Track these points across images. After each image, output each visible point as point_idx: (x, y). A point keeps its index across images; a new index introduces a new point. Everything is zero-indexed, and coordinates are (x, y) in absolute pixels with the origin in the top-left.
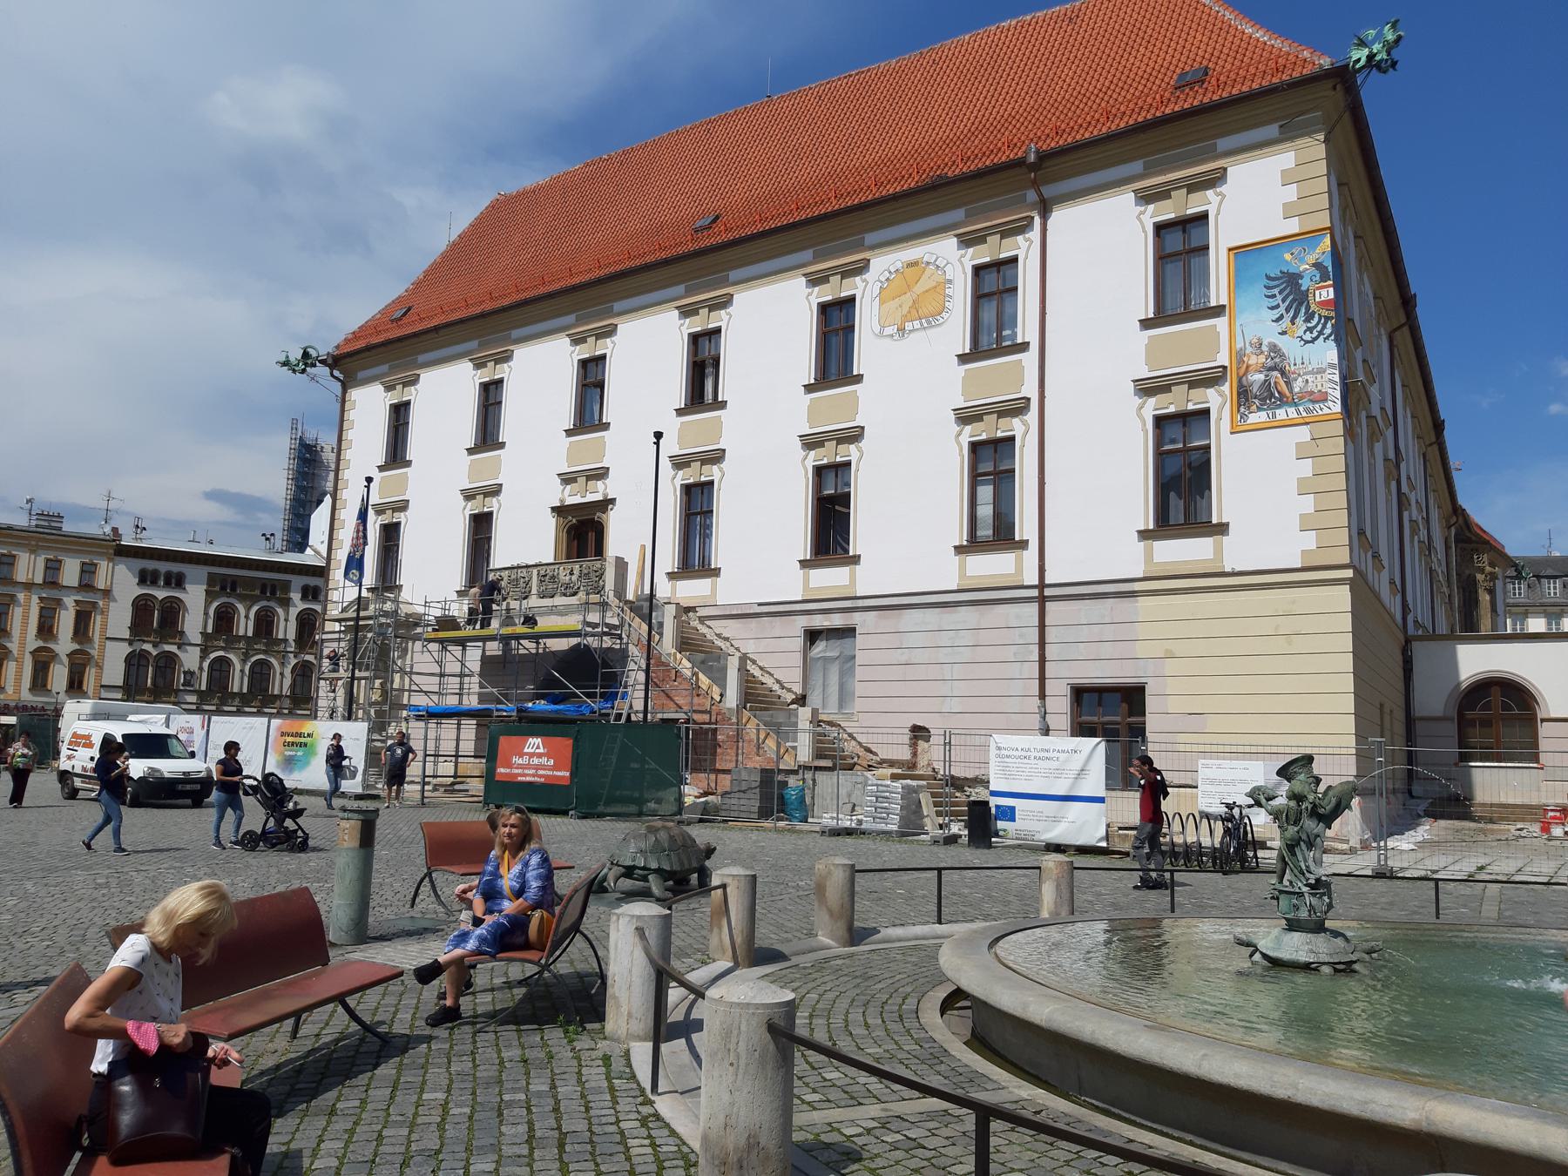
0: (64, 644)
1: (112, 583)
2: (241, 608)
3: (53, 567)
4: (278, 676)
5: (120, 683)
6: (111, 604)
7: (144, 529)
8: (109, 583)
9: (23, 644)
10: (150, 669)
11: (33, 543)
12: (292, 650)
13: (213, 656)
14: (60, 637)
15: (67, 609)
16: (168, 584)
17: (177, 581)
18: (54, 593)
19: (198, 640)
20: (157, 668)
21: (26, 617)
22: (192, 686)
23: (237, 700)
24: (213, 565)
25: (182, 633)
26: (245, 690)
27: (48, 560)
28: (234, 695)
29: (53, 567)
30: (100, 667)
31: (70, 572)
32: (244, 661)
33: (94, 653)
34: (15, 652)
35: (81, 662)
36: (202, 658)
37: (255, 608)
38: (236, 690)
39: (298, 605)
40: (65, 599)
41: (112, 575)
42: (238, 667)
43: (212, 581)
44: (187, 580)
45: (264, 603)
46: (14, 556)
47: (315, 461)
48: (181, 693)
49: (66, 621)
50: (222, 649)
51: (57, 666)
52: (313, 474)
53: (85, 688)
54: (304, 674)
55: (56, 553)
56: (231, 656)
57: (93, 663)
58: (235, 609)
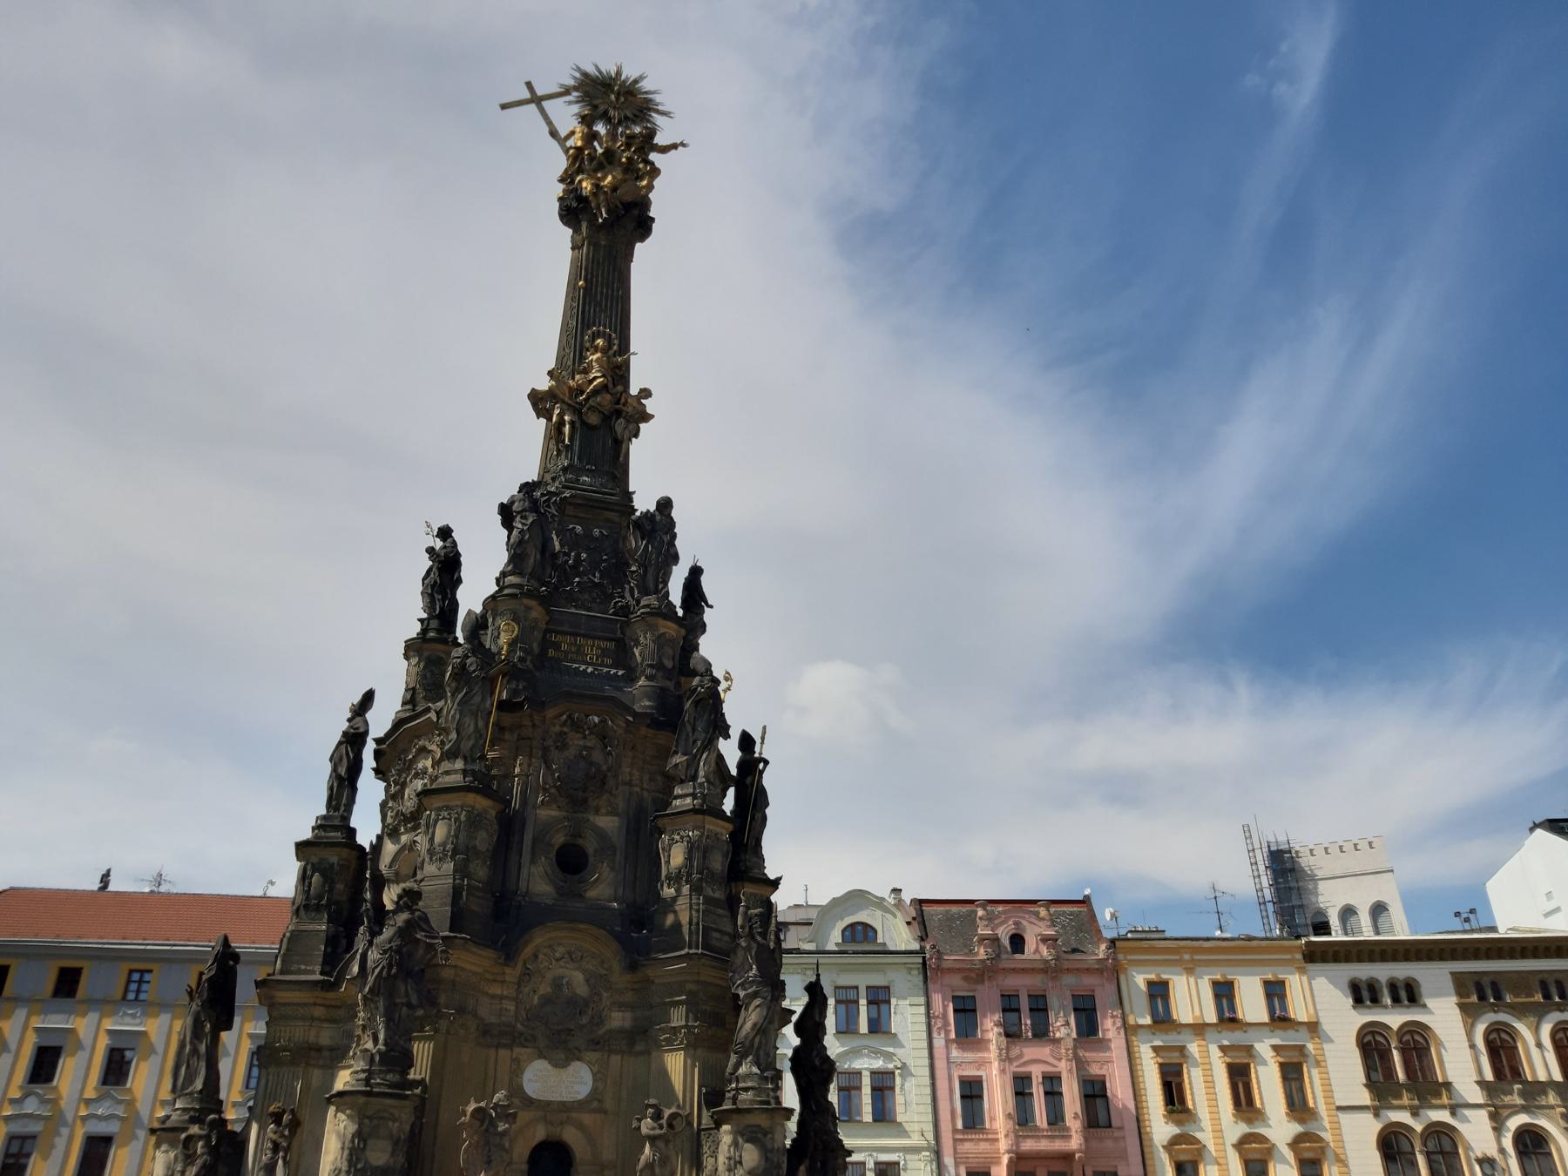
2: (1521, 1027)
3: (1224, 992)
6: (1326, 1046)
9: (1218, 1132)
11: (1187, 957)
15: (1265, 1063)
19: (1476, 1095)
21: (1210, 1083)
25: (1447, 1085)
29: (1224, 992)
31: (1251, 1003)
33: (1327, 1136)
34: (1211, 1147)
36: (1498, 1129)
43: (1462, 984)
47: (1293, 870)
55: (1225, 970)
56: (1543, 1122)
58: (1513, 1034)
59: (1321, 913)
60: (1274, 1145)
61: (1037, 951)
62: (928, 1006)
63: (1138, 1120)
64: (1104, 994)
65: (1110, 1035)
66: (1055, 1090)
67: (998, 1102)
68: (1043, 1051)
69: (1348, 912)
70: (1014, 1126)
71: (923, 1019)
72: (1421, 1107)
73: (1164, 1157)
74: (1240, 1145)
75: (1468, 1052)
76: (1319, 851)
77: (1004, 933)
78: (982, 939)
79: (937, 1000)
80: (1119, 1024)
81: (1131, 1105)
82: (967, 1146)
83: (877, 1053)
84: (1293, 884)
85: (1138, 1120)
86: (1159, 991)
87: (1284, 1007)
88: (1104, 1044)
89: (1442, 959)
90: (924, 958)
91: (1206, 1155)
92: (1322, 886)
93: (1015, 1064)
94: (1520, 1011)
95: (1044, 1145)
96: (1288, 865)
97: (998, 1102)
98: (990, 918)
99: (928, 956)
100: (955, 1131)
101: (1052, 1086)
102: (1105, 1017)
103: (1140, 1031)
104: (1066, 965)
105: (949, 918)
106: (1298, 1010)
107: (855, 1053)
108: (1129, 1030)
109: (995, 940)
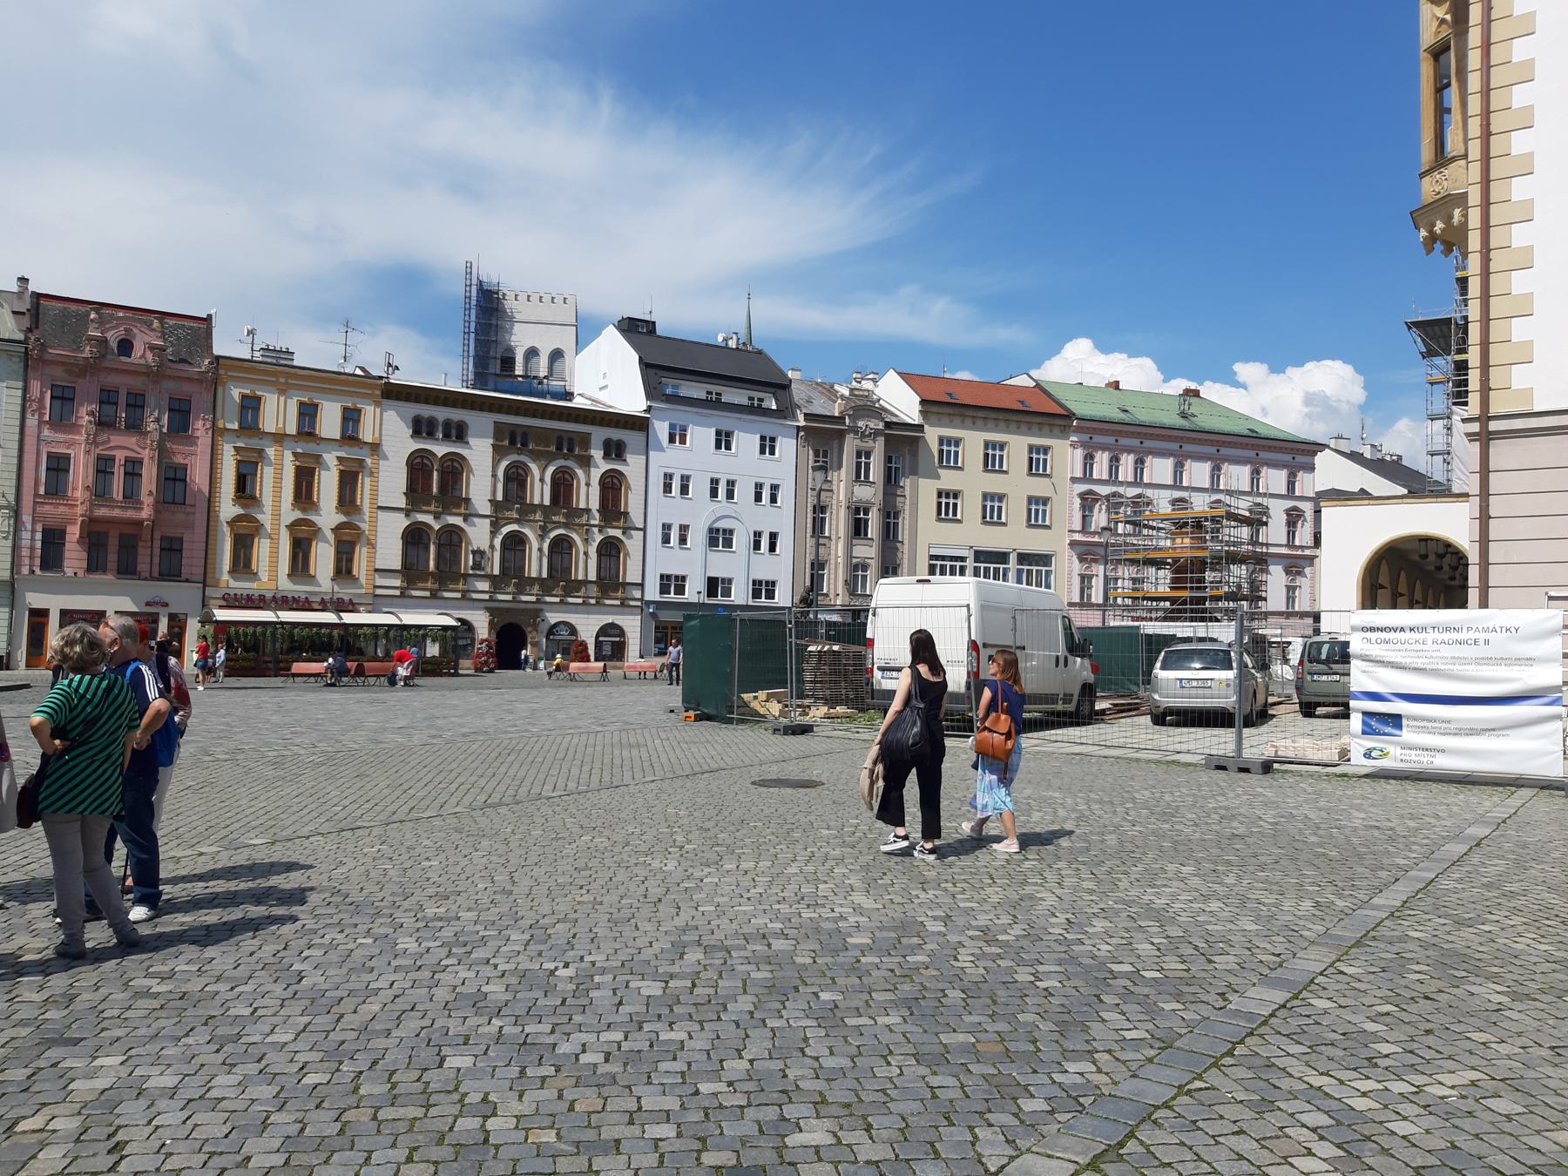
0: (328, 516)
1: (380, 434)
2: (534, 468)
3: (308, 413)
4: (582, 556)
5: (397, 565)
6: (381, 462)
7: (397, 368)
8: (377, 435)
9: (277, 515)
10: (432, 548)
12: (597, 522)
13: (505, 530)
14: (322, 504)
15: (328, 469)
16: (447, 436)
17: (457, 433)
18: (311, 448)
19: (486, 509)
20: (439, 546)
21: (278, 479)
22: (483, 569)
23: (536, 587)
24: (499, 411)
25: (468, 500)
26: (545, 575)
27: (301, 404)
28: (532, 581)
29: (308, 413)
30: (372, 545)
32: (542, 538)
33: (365, 526)
34: (268, 526)
35: (348, 538)
36: (493, 534)
37: (551, 469)
38: (534, 575)
39: (601, 466)
40: (325, 455)
41: (381, 425)
42: (535, 544)
43: (499, 431)
44: (469, 432)
45: (561, 462)
46: (259, 399)
47: (497, 309)
48: (470, 580)
49: (327, 484)
50: (517, 521)
51: (320, 544)
52: (497, 325)
53: (355, 572)
54: (611, 551)
56: (527, 531)
57: (364, 539)
58: (527, 470)
59: (511, 350)
60: (320, 529)
61: (143, 356)
62: (25, 390)
63: (209, 501)
64: (200, 398)
65: (198, 434)
66: (136, 471)
67: (80, 475)
68: (131, 441)
69: (532, 353)
70: (91, 495)
71: (19, 401)
72: (443, 513)
73: (226, 529)
74: (291, 527)
75: (490, 479)
76: (523, 297)
77: (113, 337)
78: (91, 339)
79: (35, 387)
80: (208, 425)
81: (206, 490)
82: (47, 508)
84: (494, 322)
85: (209, 501)
86: (251, 405)
87: (356, 429)
88: (192, 440)
89: (490, 410)
90: (26, 348)
91: (262, 531)
92: (517, 327)
93: (101, 448)
94: (536, 456)
95: (117, 513)
96: (495, 306)
97: (80, 475)
98: (101, 322)
99: (30, 347)
100: (36, 495)
101: (133, 470)
102: (197, 418)
103: (226, 433)
104: (168, 372)
105: (65, 314)
106: (367, 433)
108: (217, 432)
109: (103, 342)
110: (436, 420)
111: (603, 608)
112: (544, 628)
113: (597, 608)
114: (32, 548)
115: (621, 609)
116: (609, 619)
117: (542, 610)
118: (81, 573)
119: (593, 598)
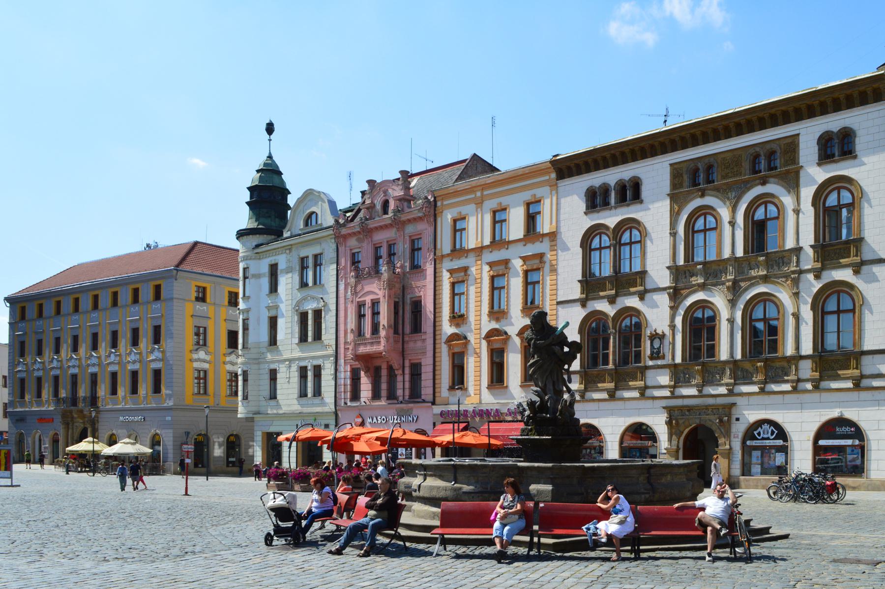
22: (663, 357)
26: (738, 356)
36: (674, 309)
48: (650, 374)
72: (617, 295)
75: (667, 240)
83: (313, 298)
107: (304, 299)
110: (609, 185)
111: (825, 396)
112: (738, 429)
113: (816, 396)
114: (345, 385)
115: (855, 395)
116: (835, 413)
117: (734, 404)
118: (368, 403)
119: (807, 380)
